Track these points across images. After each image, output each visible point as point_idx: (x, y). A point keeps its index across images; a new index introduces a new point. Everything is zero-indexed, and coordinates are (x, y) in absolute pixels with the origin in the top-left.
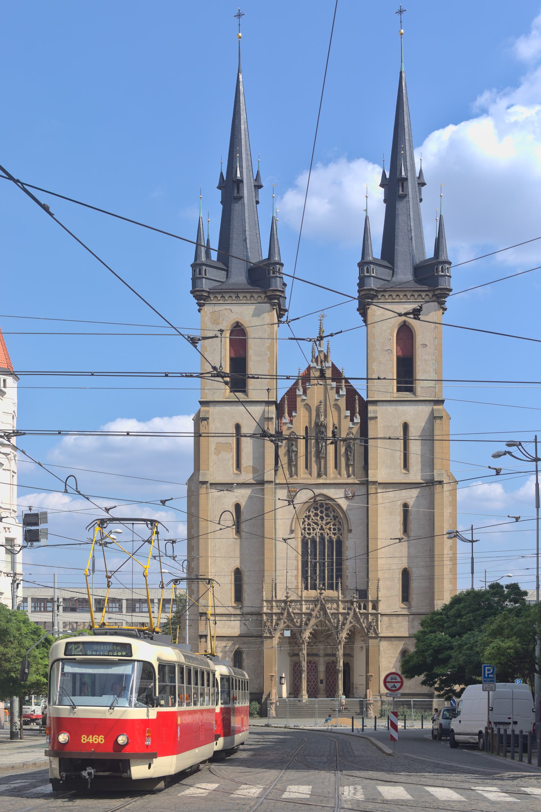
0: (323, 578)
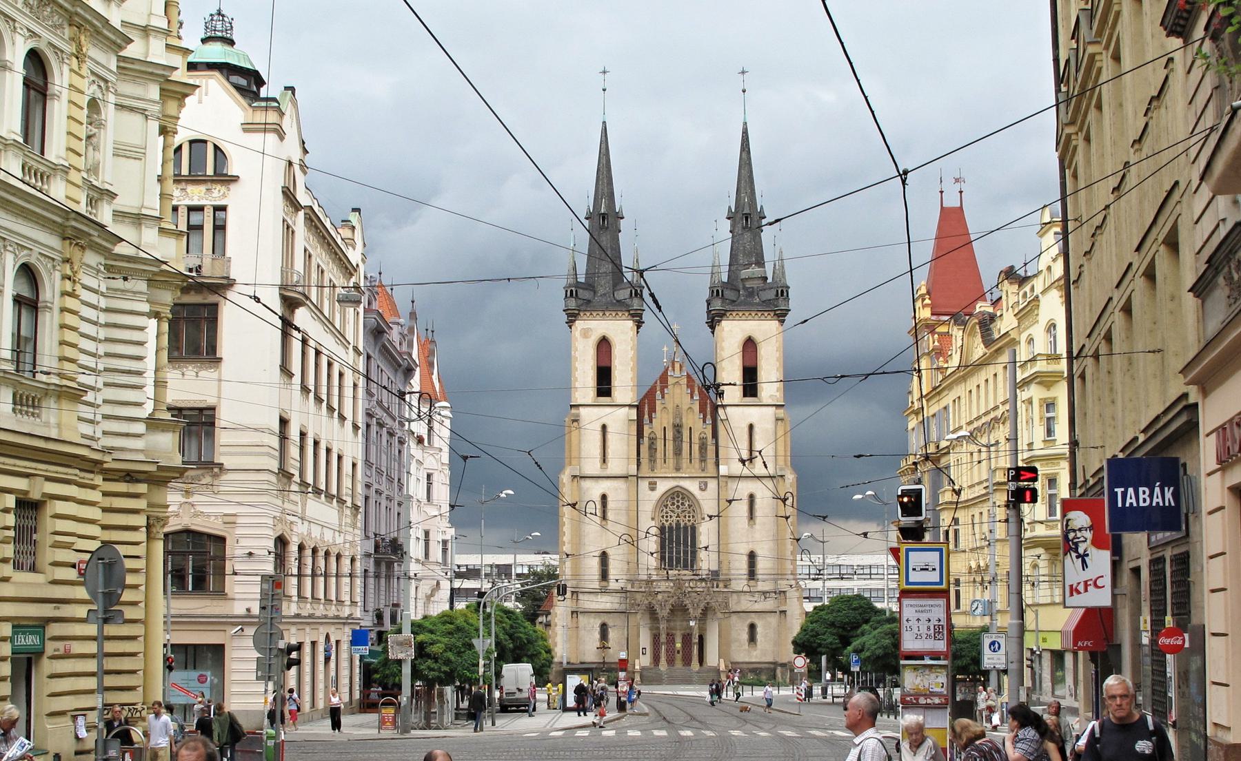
0: (678, 561)
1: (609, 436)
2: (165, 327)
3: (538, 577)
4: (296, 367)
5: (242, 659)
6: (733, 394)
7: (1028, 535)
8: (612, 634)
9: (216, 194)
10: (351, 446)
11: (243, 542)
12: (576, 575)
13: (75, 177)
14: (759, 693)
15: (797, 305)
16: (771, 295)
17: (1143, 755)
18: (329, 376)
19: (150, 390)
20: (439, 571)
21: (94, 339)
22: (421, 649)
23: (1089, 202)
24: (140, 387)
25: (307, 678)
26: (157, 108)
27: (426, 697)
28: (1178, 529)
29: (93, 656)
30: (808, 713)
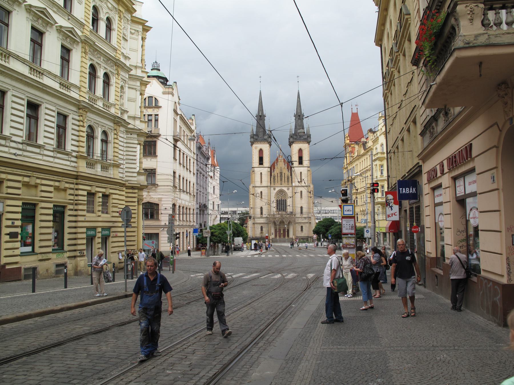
1: (263, 176)
2: (142, 147)
3: (244, 214)
4: (178, 158)
5: (164, 237)
6: (296, 164)
7: (376, 201)
8: (264, 229)
9: (155, 111)
10: (193, 179)
11: (164, 205)
12: (254, 213)
13: (117, 107)
14: (304, 245)
15: (313, 139)
16: (306, 137)
17: (408, 260)
18: (187, 160)
19: (138, 164)
20: (217, 212)
21: (123, 151)
22: (212, 234)
23: (392, 111)
24: (135, 164)
25: (181, 242)
26: (139, 88)
27: (214, 246)
28: (417, 199)
29: (123, 237)
30: (317, 250)
